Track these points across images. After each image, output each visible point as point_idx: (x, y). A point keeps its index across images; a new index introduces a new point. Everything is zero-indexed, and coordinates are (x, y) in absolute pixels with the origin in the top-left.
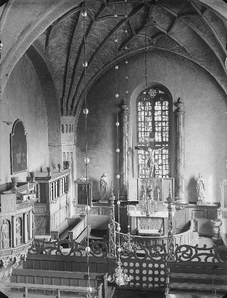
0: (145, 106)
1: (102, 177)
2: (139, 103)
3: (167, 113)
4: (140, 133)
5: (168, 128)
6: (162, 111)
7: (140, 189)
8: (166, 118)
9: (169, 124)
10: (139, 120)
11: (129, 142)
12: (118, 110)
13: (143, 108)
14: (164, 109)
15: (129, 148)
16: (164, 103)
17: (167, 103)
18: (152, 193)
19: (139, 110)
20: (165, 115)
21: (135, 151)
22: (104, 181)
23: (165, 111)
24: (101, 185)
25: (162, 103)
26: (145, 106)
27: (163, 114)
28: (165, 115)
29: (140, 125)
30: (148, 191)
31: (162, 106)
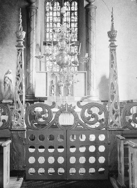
0: (53, 6)
1: (6, 74)
2: (48, 3)
3: (76, 14)
4: (48, 35)
5: (76, 29)
6: (71, 12)
7: (49, 84)
8: (76, 19)
9: (78, 25)
10: (48, 20)
11: (36, 38)
12: (27, 4)
13: (51, 8)
14: (73, 10)
15: (37, 45)
16: (73, 3)
17: (76, 3)
18: (62, 89)
19: (48, 10)
20: (74, 16)
21: (43, 46)
22: (8, 78)
23: (74, 11)
24: (5, 83)
25: (71, 3)
26: (53, 6)
27: (73, 14)
28: (74, 16)
29: (48, 26)
30: (59, 87)
31: (71, 6)
